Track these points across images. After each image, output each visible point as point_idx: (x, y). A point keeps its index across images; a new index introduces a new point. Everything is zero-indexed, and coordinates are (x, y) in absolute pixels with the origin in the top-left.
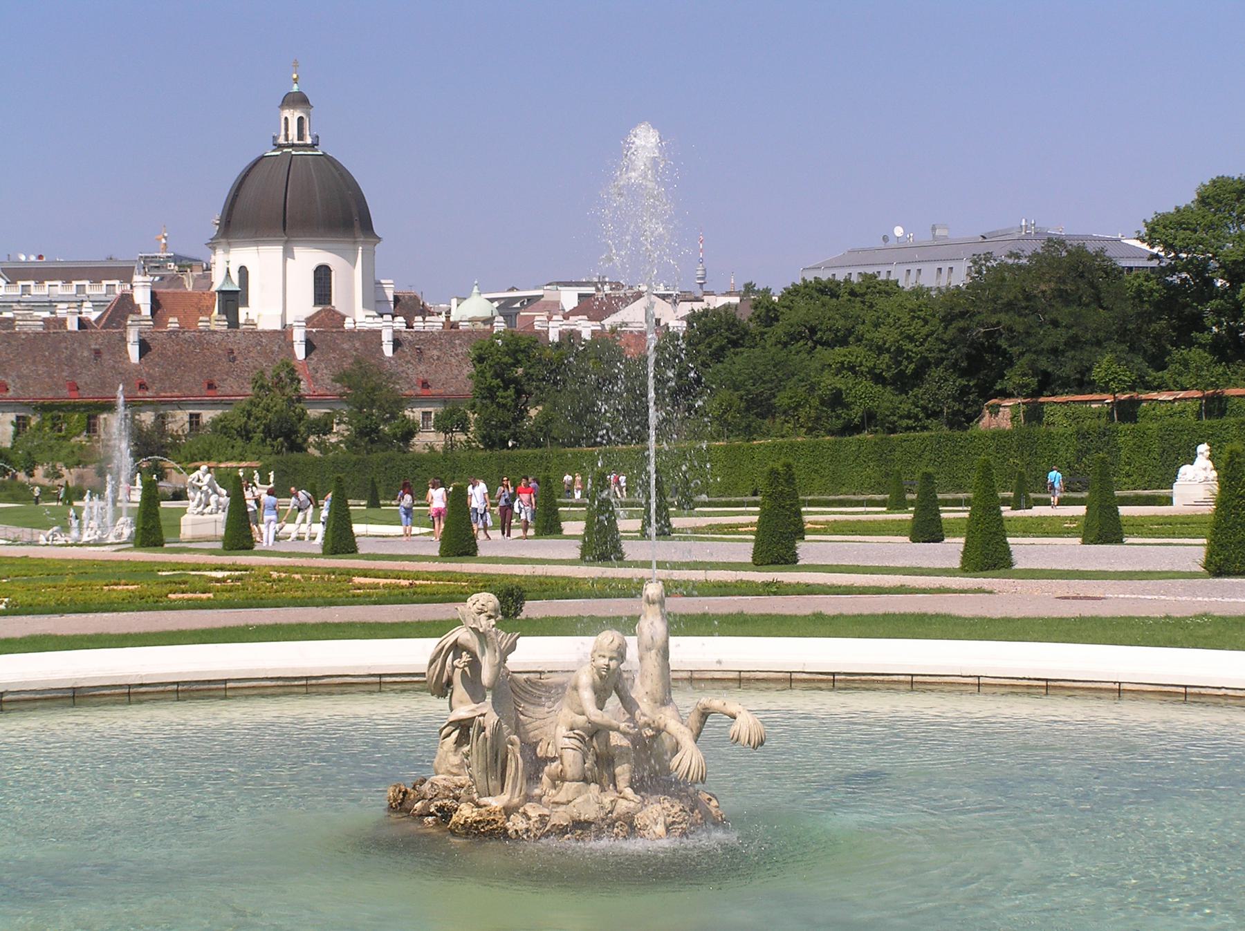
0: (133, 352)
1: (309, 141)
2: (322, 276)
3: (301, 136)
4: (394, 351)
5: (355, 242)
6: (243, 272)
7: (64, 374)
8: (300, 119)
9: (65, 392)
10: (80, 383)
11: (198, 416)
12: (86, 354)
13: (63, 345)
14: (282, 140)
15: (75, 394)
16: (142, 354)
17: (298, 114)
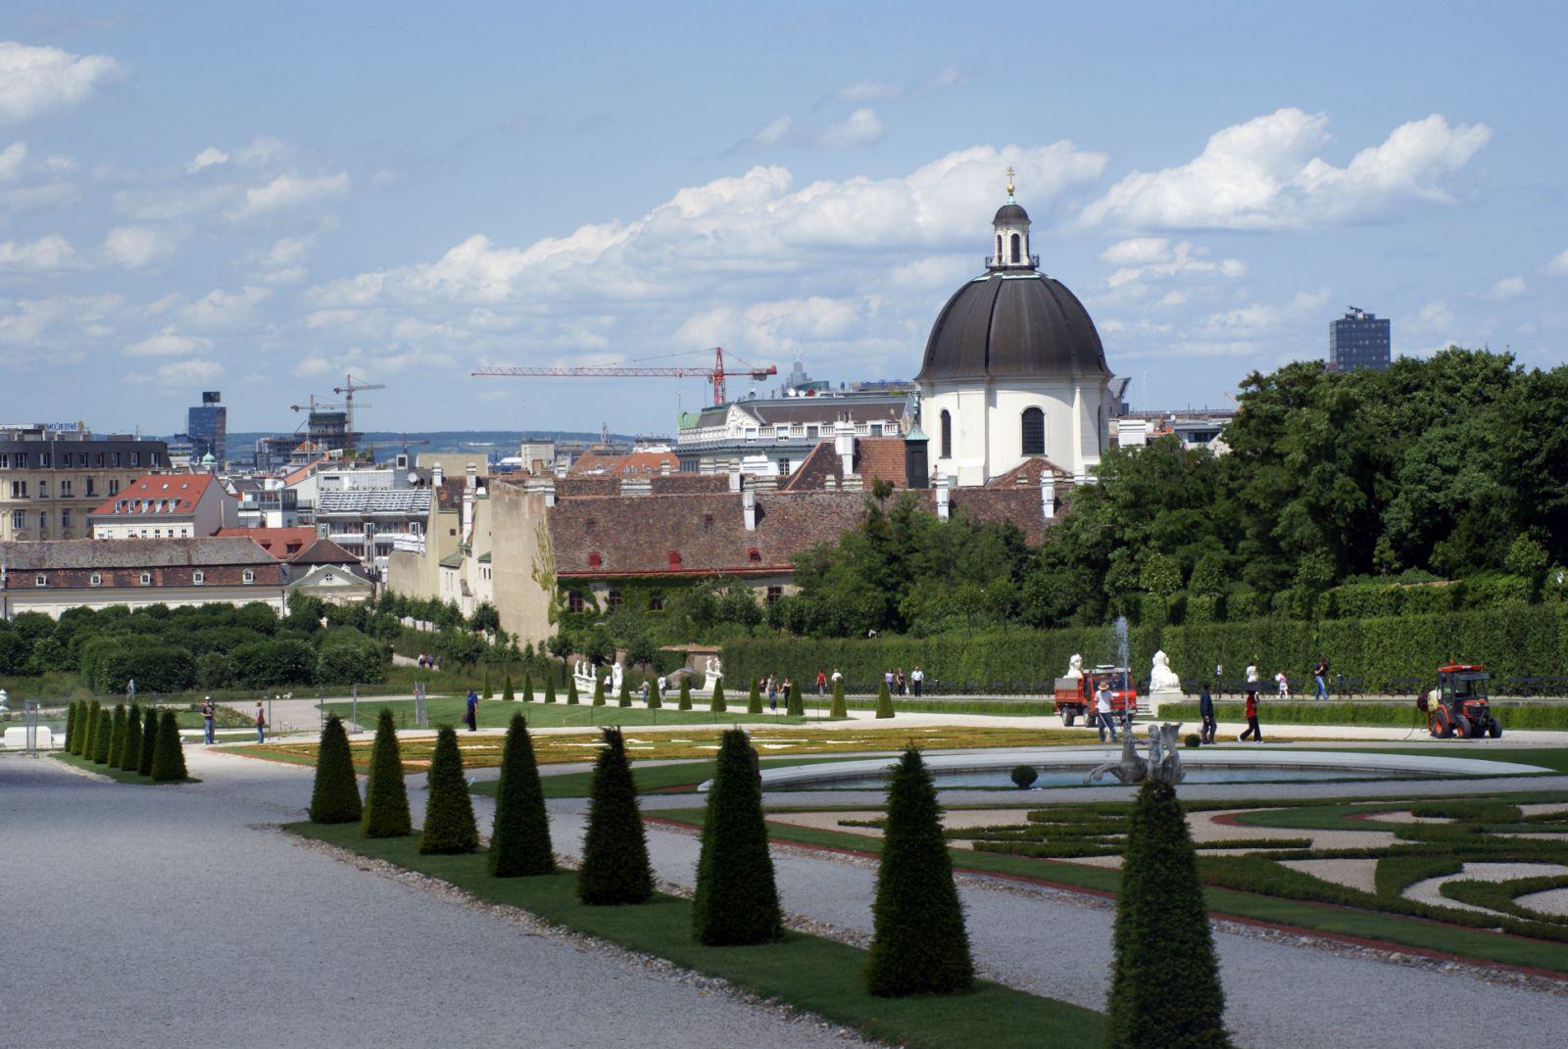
0: (749, 517)
1: (1025, 262)
2: (1033, 421)
3: (1016, 257)
4: (1055, 511)
5: (1073, 380)
6: (945, 416)
7: (668, 544)
8: (1015, 239)
9: (665, 565)
10: (683, 553)
11: (779, 590)
12: (696, 520)
13: (671, 511)
14: (995, 263)
15: (676, 567)
16: (758, 519)
17: (1012, 232)
